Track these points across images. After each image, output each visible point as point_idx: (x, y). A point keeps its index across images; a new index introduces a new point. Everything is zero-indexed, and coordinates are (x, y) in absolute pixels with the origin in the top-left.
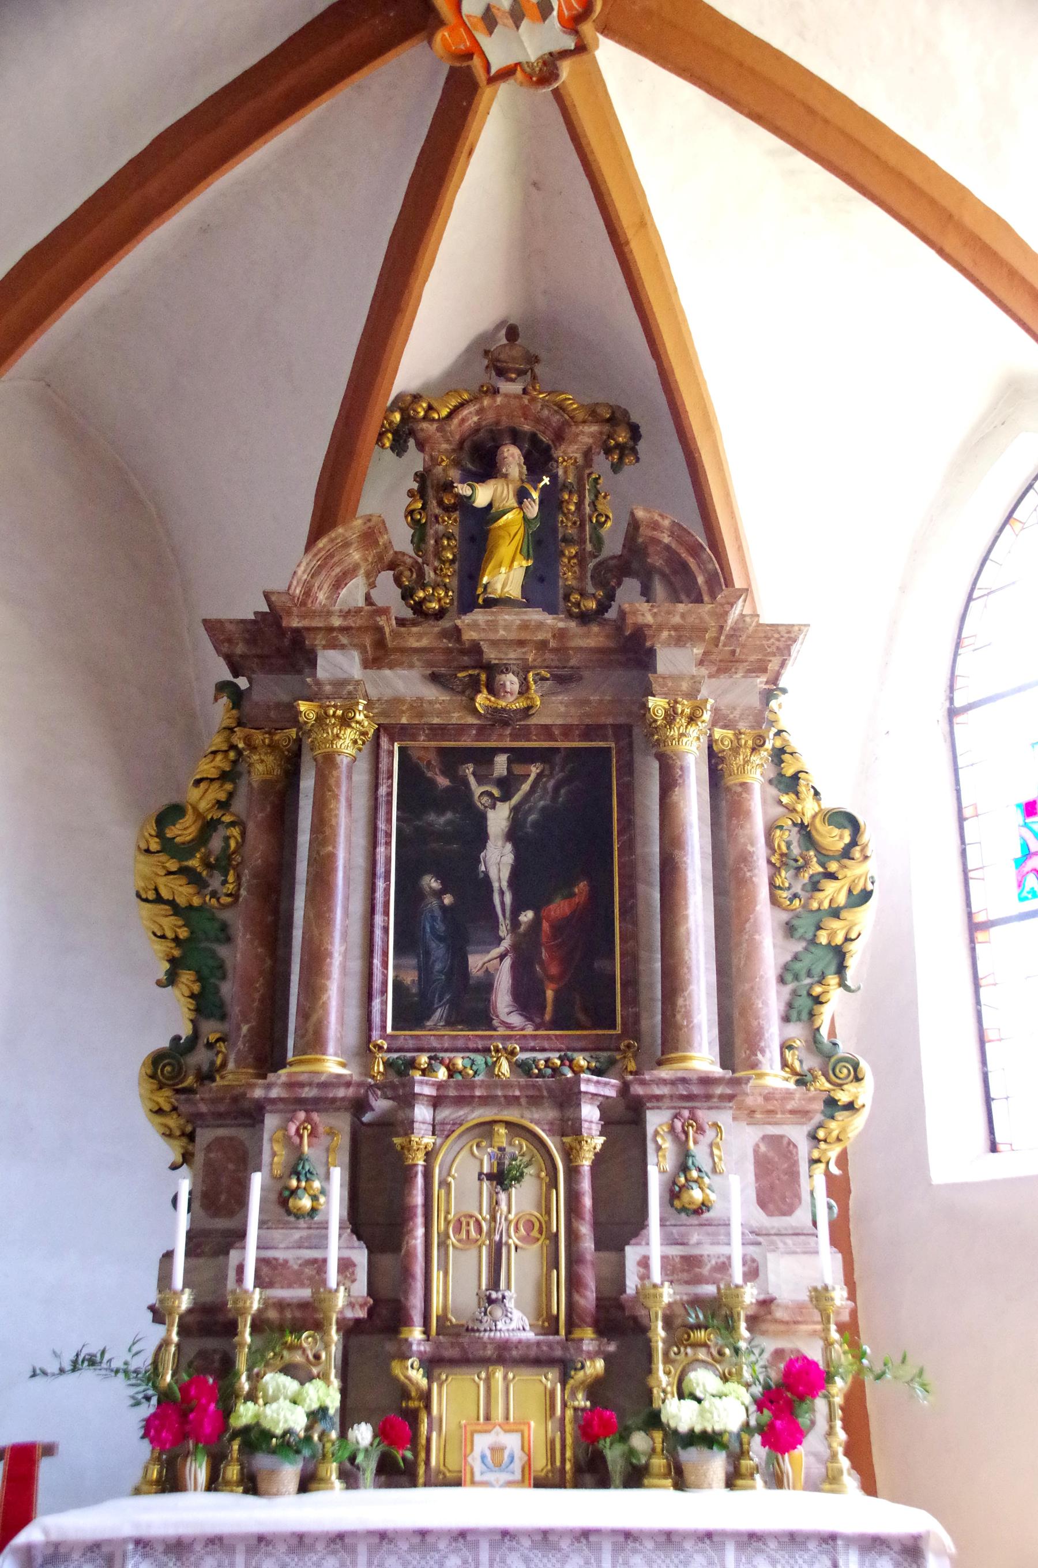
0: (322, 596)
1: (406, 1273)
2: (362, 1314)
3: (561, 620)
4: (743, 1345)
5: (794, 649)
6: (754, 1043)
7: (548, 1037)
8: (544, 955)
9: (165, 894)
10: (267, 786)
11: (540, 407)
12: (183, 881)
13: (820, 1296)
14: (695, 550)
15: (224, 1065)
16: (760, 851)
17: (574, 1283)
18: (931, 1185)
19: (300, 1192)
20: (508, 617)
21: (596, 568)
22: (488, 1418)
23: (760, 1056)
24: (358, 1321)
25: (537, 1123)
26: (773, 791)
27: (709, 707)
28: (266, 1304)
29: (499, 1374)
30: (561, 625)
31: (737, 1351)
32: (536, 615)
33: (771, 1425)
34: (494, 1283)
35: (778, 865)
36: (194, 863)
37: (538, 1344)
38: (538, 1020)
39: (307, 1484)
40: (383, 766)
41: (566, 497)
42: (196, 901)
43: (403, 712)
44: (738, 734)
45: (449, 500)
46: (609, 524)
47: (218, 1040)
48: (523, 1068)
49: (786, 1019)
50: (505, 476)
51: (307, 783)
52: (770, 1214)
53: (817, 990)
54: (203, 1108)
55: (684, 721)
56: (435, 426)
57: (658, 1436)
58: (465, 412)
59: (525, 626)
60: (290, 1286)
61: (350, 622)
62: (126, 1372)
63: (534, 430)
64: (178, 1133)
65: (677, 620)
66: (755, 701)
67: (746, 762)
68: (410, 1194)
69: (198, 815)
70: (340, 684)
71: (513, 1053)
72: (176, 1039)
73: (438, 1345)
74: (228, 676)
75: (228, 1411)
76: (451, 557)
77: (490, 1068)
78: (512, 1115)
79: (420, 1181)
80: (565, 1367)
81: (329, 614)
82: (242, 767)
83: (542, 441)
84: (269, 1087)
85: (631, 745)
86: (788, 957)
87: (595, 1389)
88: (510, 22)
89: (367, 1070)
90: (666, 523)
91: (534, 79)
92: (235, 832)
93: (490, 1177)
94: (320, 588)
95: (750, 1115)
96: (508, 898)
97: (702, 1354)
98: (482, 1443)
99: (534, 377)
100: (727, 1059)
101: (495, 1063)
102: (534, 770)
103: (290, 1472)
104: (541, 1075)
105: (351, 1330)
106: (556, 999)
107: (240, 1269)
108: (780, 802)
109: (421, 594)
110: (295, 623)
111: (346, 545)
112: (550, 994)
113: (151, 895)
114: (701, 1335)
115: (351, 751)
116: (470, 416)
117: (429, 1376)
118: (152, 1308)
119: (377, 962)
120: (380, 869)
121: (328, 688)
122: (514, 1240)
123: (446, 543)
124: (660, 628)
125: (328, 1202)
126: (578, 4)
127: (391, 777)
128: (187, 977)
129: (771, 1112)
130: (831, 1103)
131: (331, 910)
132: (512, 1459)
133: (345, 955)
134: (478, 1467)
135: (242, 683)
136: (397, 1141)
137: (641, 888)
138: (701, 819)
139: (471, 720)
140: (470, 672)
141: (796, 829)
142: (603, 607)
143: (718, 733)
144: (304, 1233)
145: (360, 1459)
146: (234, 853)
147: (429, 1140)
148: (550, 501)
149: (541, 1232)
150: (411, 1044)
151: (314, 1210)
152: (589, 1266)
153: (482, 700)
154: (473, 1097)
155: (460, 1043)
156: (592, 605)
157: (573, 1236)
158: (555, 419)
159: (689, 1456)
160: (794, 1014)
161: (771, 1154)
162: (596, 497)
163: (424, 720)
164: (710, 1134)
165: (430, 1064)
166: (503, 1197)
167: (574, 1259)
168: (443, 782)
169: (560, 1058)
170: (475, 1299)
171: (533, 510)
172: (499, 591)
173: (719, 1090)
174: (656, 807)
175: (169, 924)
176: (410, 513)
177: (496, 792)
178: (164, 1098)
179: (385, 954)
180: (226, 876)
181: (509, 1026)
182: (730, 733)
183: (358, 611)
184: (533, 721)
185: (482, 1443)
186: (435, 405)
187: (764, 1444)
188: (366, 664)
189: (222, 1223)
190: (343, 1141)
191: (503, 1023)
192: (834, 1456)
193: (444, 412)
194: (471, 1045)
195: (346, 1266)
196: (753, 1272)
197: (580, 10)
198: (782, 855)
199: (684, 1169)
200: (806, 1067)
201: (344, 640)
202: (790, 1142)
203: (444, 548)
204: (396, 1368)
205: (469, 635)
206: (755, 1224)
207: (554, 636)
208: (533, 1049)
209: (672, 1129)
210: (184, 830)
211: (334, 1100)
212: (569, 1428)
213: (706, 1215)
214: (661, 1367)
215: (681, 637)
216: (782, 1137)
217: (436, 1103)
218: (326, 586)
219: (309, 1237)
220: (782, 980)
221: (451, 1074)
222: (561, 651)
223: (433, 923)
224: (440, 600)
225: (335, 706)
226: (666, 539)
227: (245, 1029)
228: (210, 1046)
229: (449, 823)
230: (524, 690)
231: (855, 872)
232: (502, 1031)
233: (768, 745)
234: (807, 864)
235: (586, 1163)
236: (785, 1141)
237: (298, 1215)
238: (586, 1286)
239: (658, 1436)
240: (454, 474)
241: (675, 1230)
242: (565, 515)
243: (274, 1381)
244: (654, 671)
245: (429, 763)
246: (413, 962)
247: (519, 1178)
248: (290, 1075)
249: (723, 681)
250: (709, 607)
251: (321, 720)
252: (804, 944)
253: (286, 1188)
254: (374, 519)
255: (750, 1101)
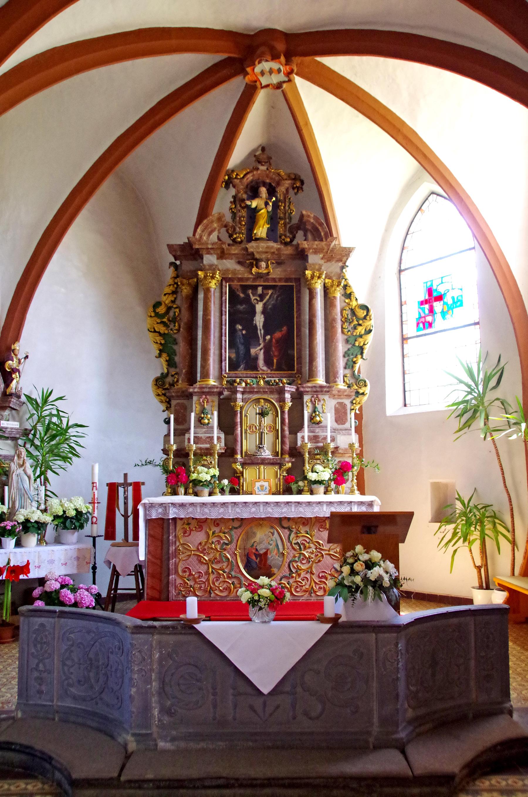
0: (205, 238)
1: (236, 440)
2: (223, 451)
3: (279, 245)
4: (330, 458)
5: (351, 255)
6: (335, 376)
7: (275, 374)
8: (273, 349)
9: (157, 330)
10: (187, 297)
11: (272, 174)
12: (162, 325)
13: (351, 446)
14: (321, 224)
15: (178, 381)
16: (339, 317)
17: (283, 443)
18: (386, 416)
19: (205, 418)
20: (263, 245)
21: (290, 227)
22: (259, 478)
23: (337, 379)
24: (222, 453)
25: (273, 399)
26: (343, 298)
27: (324, 274)
28: (197, 448)
29: (262, 467)
30: (279, 246)
31: (328, 460)
32: (271, 244)
33: (337, 479)
34: (261, 443)
35: (345, 320)
36: (165, 320)
37: (273, 459)
38: (271, 368)
39: (210, 494)
40: (224, 291)
41: (280, 204)
42: (166, 332)
43: (230, 274)
45: (243, 205)
46: (294, 213)
47: (175, 374)
48: (267, 383)
49: (345, 368)
50: (261, 197)
51: (201, 296)
52: (339, 424)
53: (355, 359)
54: (173, 394)
55: (317, 278)
56: (239, 180)
57: (306, 482)
58: (248, 176)
59: (268, 247)
60: (203, 444)
61: (214, 247)
62: (160, 465)
63: (270, 182)
64: (164, 401)
65: (315, 246)
66: (338, 270)
67: (335, 290)
68: (236, 419)
69: (166, 305)
70: (211, 266)
71: (264, 378)
72: (162, 374)
73: (245, 460)
74: (173, 260)
75: (189, 476)
76: (244, 223)
77: (258, 383)
78: (265, 396)
79: (239, 415)
80: (281, 465)
81: (207, 244)
82: (179, 290)
83: (272, 186)
84: (195, 388)
85: (300, 284)
86: (346, 349)
87: (288, 471)
89: (221, 383)
90: (312, 215)
92: (177, 310)
93: (259, 414)
94: (204, 236)
95: (333, 396)
96: (262, 332)
97: (318, 462)
98: (258, 484)
99: (270, 164)
100: (327, 381)
101: (259, 381)
102: (270, 292)
103: (206, 491)
104: (273, 385)
105: (220, 455)
106: (276, 363)
107: (189, 439)
108: (345, 302)
109: (235, 236)
110: (197, 247)
111: (212, 222)
112: (275, 361)
113: (153, 330)
114: (318, 457)
115: (214, 287)
116: (250, 177)
117: (243, 467)
118: (162, 450)
119: (223, 351)
120: (224, 323)
121: (207, 267)
122: (266, 431)
123: (242, 219)
124: (310, 249)
125: (213, 421)
127: (226, 294)
128: (164, 355)
130: (357, 393)
131: (210, 336)
132: (266, 488)
133: (214, 349)
134: (257, 490)
135: (178, 262)
136: (232, 404)
137: (303, 329)
138: (321, 307)
139: (251, 276)
140: (250, 261)
141: (350, 310)
142: (292, 241)
143: (327, 281)
144: (206, 429)
145: (225, 488)
146: (177, 317)
147: (241, 404)
148: (276, 206)
149: (273, 429)
150: (234, 375)
151: (208, 423)
152: (287, 438)
153: (254, 270)
154: (254, 391)
155: (248, 375)
156: (289, 240)
157: (283, 430)
158: (277, 178)
159: (314, 487)
160: (347, 366)
161: (339, 407)
162: (290, 204)
163: (236, 276)
164: (322, 402)
165: (240, 382)
166: (263, 419)
167: (283, 436)
168: (242, 295)
169: (278, 380)
170: (255, 447)
171: (270, 209)
172: (259, 235)
173: (325, 390)
174: (308, 304)
175: (159, 339)
176: (231, 209)
177: (258, 299)
178: (160, 391)
179: (226, 348)
180: (175, 324)
181: (264, 371)
182: (330, 281)
183: (216, 243)
184: (270, 276)
185: (258, 484)
186: (239, 173)
187: (334, 483)
188: (218, 259)
189: (181, 427)
190: (216, 404)
191: (261, 369)
192: (353, 486)
193: (242, 176)
194: (252, 376)
195: (219, 438)
196: (333, 440)
198: (345, 318)
199: (315, 412)
200: (350, 382)
201: (212, 252)
202: (345, 404)
203: (242, 221)
204: (234, 466)
205: (250, 250)
206: (334, 427)
207: (277, 250)
208: (270, 377)
209: (311, 401)
210: (162, 310)
211: (213, 392)
212: (281, 481)
213: (320, 425)
214: (307, 464)
215: (316, 252)
217: (243, 393)
218: (206, 235)
219: (207, 430)
220: (344, 356)
221: (246, 385)
222: (279, 255)
223: (239, 340)
224: (241, 238)
225: (210, 273)
226: (312, 221)
227: (184, 371)
228: (172, 376)
229: (244, 308)
230: (267, 267)
231: (368, 324)
232: (260, 372)
233: (342, 285)
234: (353, 321)
235: (286, 410)
236: (344, 404)
237: (204, 424)
238: (286, 444)
239: (306, 482)
240: (245, 196)
241: (312, 428)
242: (280, 210)
243: (200, 468)
244: (308, 262)
245: (238, 289)
246: (234, 351)
247: (267, 414)
248: (200, 385)
249: (329, 264)
250: (325, 243)
251: (205, 277)
252: (351, 345)
253: (201, 417)
254: (221, 214)
255: (334, 392)
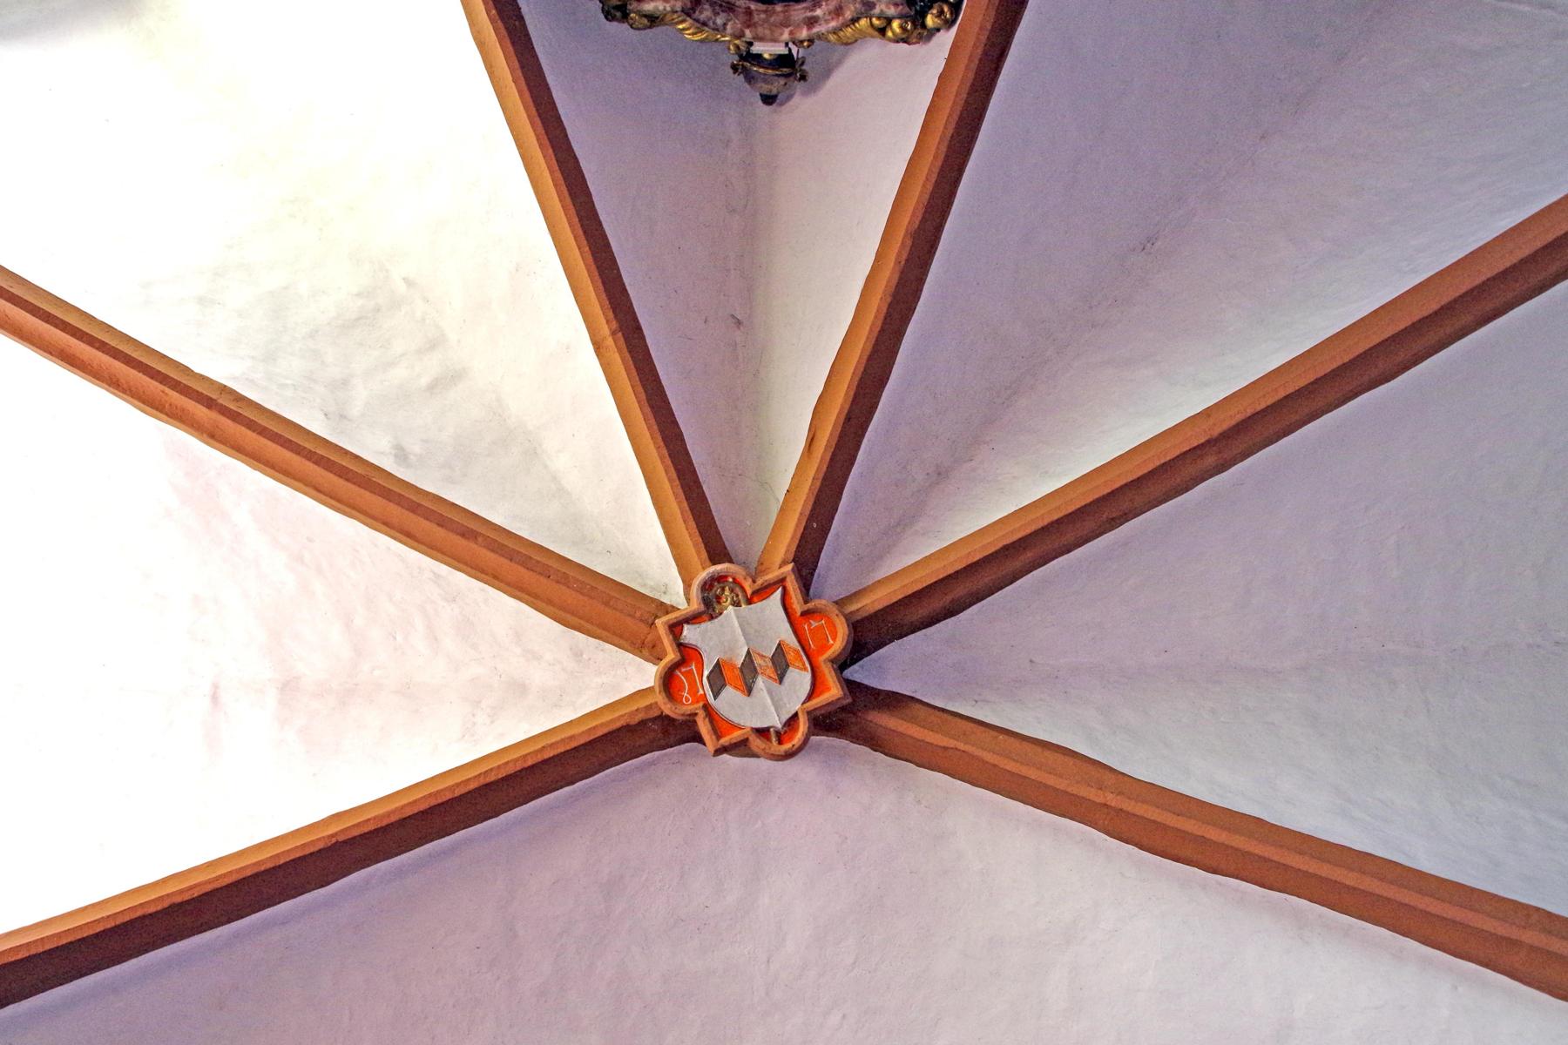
11: (729, 27)
88: (758, 661)
91: (731, 580)
126: (678, 676)
193: (863, 22)
197: (678, 673)
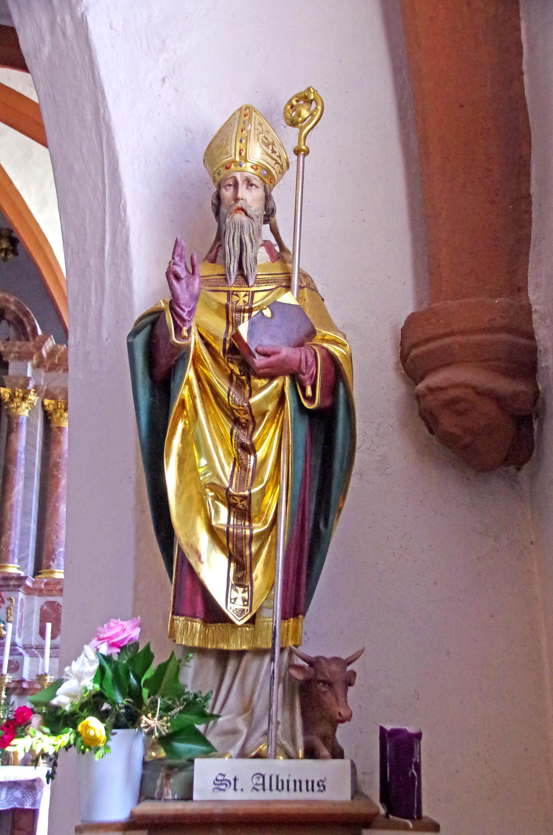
6: (51, 556)
44: (57, 403)
65: (16, 349)
124: (10, 352)
129: (50, 591)
161: (48, 610)
182: (53, 402)
202: (59, 605)
215: (24, 357)
216: (55, 602)
226: (13, 307)
236: (56, 604)
244: (7, 373)
249: (53, 374)
250: (32, 343)
